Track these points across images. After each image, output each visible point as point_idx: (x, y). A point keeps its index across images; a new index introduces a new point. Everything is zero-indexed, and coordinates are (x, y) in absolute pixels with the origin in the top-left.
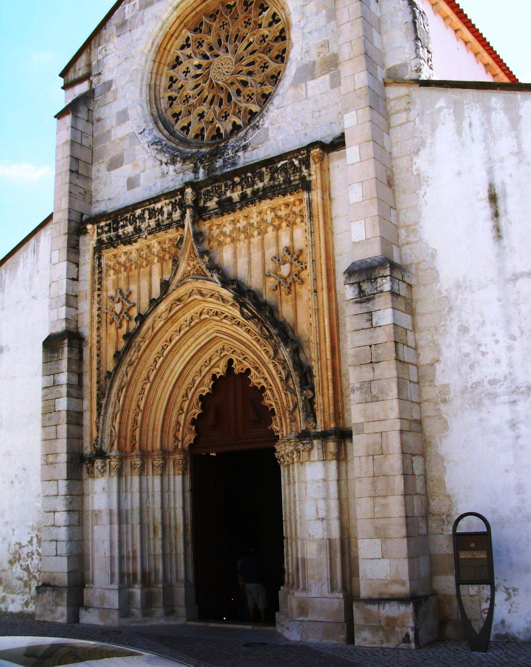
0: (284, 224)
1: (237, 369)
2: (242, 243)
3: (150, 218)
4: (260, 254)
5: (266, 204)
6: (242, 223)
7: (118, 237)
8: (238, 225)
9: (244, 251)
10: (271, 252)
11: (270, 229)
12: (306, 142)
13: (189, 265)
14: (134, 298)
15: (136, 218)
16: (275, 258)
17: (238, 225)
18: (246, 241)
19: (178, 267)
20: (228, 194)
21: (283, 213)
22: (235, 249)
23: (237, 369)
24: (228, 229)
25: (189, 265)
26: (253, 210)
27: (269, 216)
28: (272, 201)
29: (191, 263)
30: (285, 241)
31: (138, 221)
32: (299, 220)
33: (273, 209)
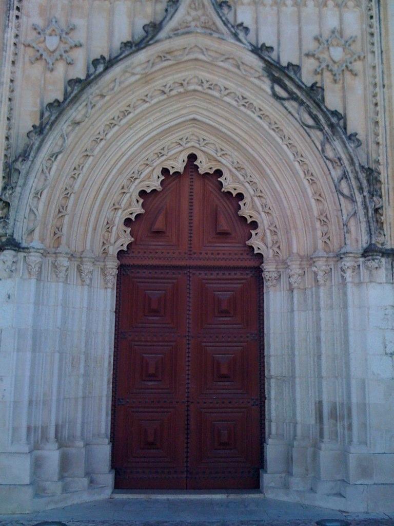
1: (204, 166)
2: (268, 9)
4: (297, 28)
10: (311, 30)
13: (188, 13)
14: (79, 36)
16: (317, 39)
18: (275, 8)
19: (176, 10)
22: (257, 12)
23: (204, 166)
25: (188, 13)
29: (193, 13)
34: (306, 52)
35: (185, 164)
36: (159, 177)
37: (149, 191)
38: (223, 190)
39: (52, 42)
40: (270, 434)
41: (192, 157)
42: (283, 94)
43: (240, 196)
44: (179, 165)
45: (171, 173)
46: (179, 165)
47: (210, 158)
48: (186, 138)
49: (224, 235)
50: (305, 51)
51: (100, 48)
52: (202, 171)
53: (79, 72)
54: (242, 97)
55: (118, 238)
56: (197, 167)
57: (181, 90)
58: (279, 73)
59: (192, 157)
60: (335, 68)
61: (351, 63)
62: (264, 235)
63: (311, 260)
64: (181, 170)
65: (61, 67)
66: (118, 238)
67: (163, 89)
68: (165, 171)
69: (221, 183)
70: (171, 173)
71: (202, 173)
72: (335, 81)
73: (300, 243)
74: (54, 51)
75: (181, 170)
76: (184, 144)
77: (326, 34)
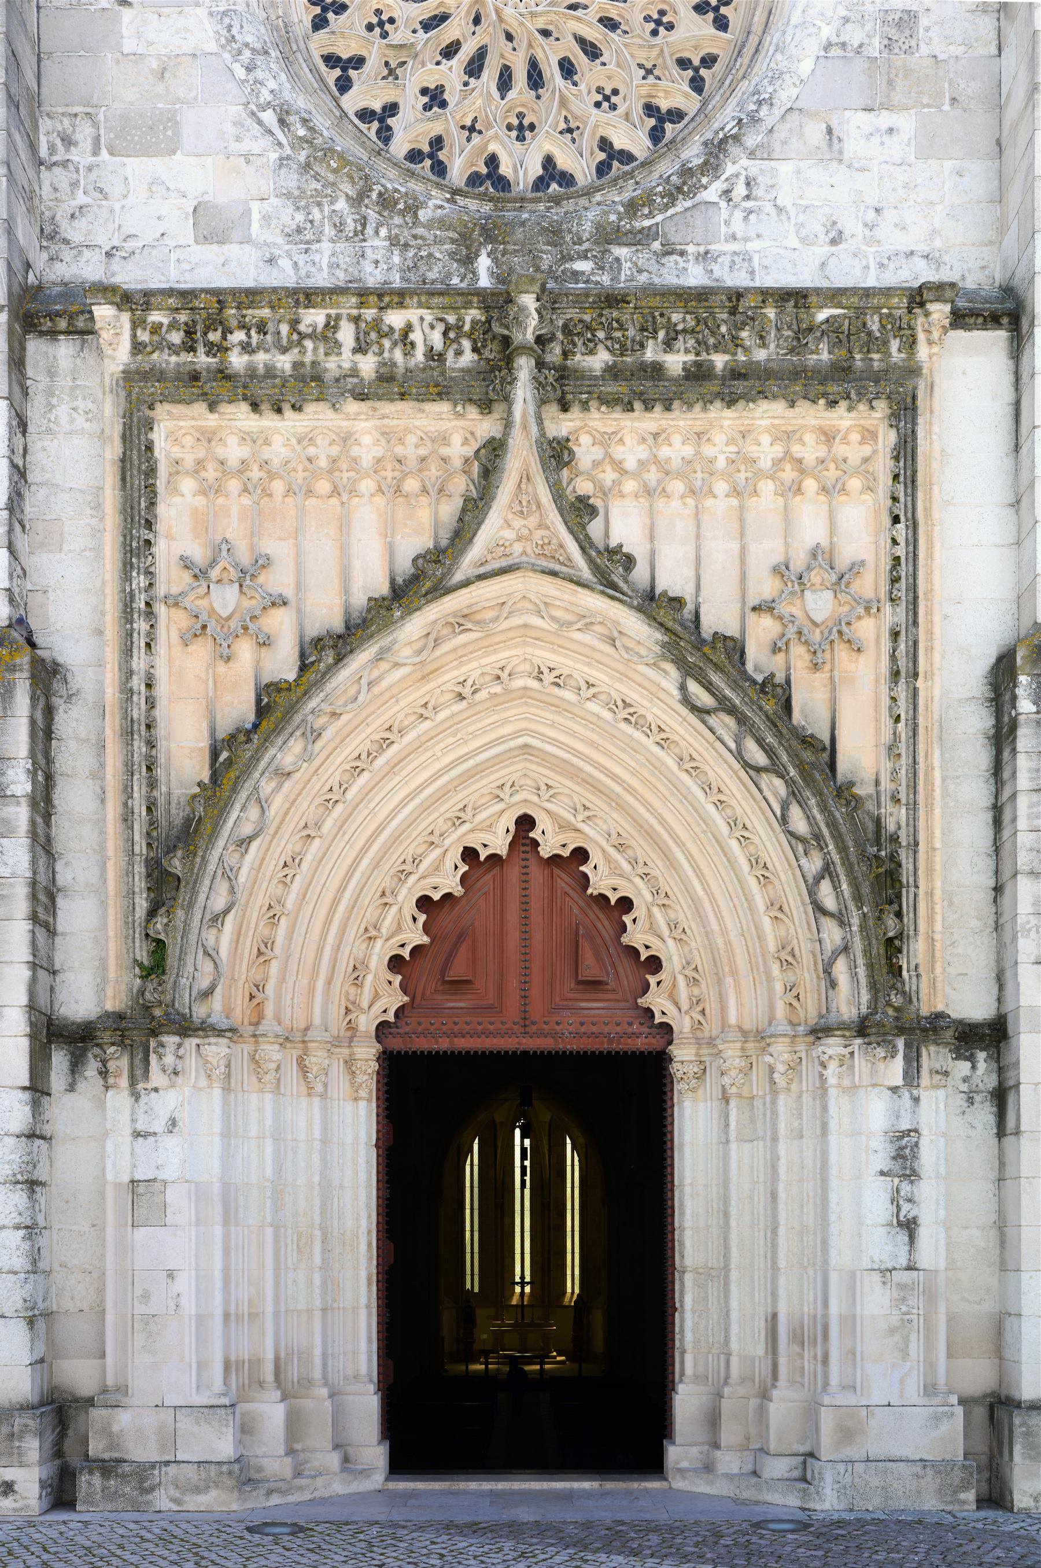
0: (810, 485)
1: (551, 842)
2: (675, 503)
3: (360, 349)
4: (736, 547)
5: (768, 414)
6: (676, 451)
7: (223, 374)
8: (664, 452)
9: (684, 526)
10: (766, 551)
11: (767, 487)
12: (922, 273)
14: (279, 580)
15: (302, 336)
16: (780, 570)
17: (664, 452)
18: (690, 501)
20: (650, 354)
21: (810, 450)
22: (651, 513)
23: (551, 842)
24: (631, 453)
26: (722, 421)
27: (766, 451)
28: (790, 413)
29: (517, 523)
30: (812, 530)
31: (309, 344)
32: (855, 484)
33: (787, 436)
34: (756, 602)
35: (510, 838)
36: (456, 867)
37: (436, 896)
38: (590, 891)
39: (226, 599)
40: (682, 1374)
41: (526, 822)
42: (705, 699)
43: (626, 904)
44: (499, 843)
45: (482, 858)
46: (499, 843)
47: (563, 826)
48: (510, 783)
49: (594, 985)
50: (753, 601)
51: (326, 613)
52: (545, 852)
53: (282, 664)
54: (624, 701)
55: (376, 997)
56: (536, 844)
57: (498, 689)
58: (697, 649)
59: (526, 822)
60: (817, 636)
61: (848, 624)
62: (674, 985)
63: (760, 1037)
64: (503, 851)
65: (245, 651)
66: (376, 997)
67: (459, 689)
68: (469, 854)
69: (585, 876)
70: (482, 858)
71: (546, 856)
72: (816, 667)
73: (744, 1003)
74: (229, 618)
75: (503, 851)
76: (506, 797)
77: (799, 562)
